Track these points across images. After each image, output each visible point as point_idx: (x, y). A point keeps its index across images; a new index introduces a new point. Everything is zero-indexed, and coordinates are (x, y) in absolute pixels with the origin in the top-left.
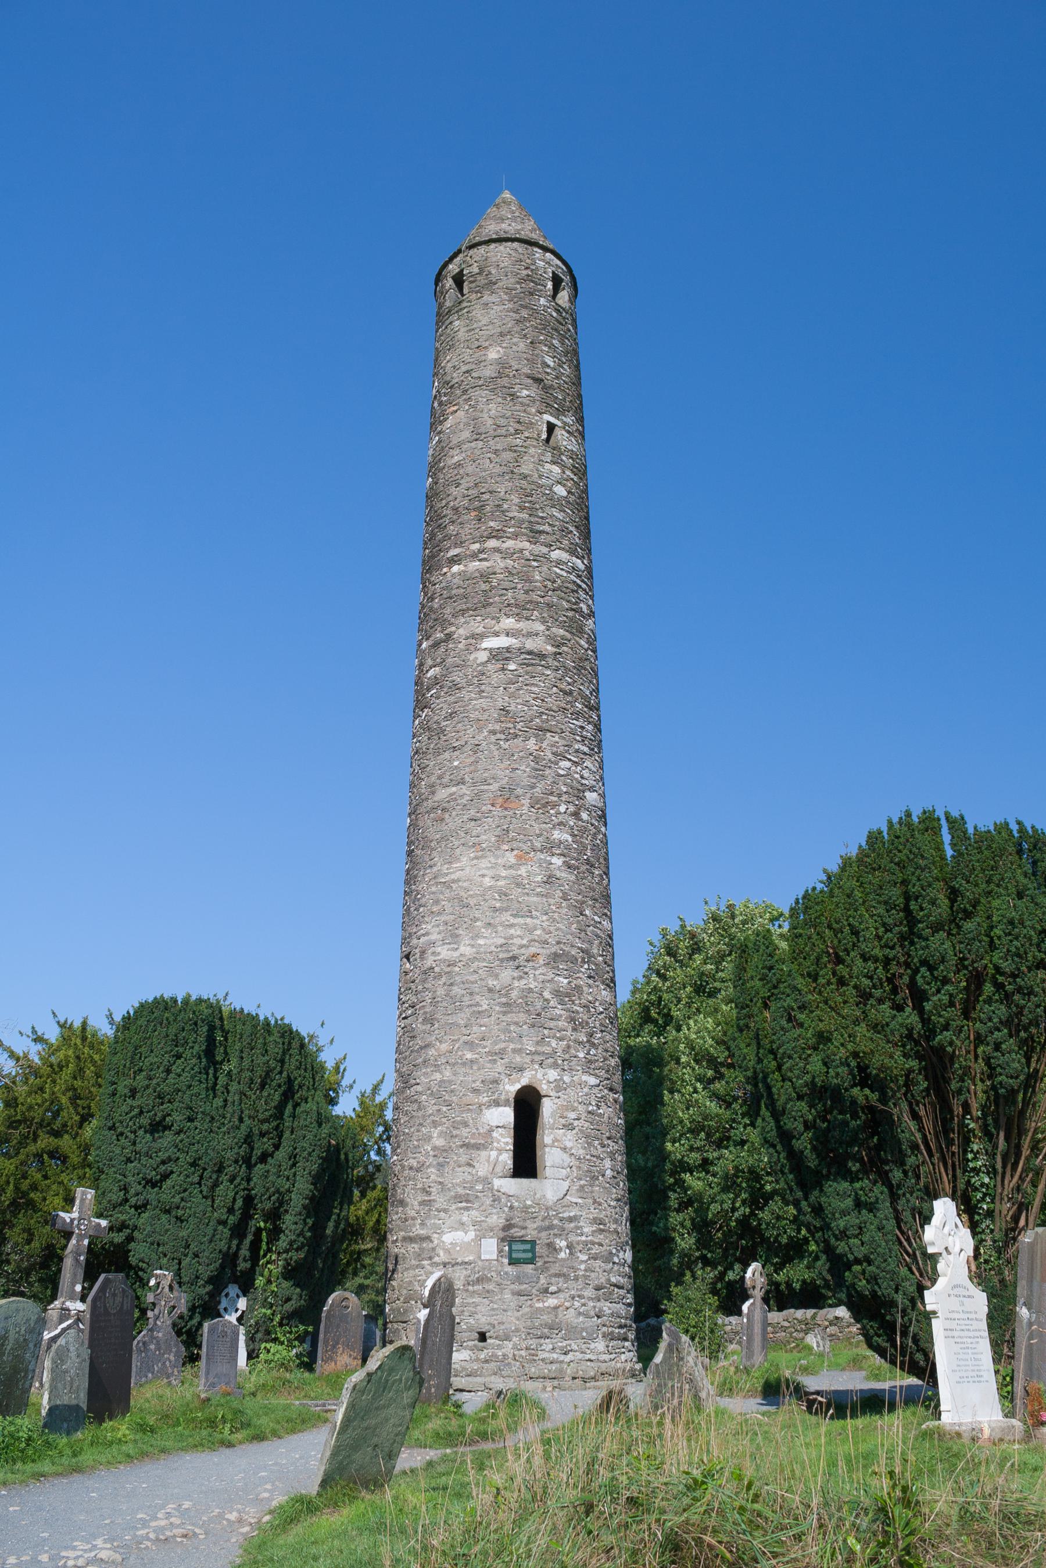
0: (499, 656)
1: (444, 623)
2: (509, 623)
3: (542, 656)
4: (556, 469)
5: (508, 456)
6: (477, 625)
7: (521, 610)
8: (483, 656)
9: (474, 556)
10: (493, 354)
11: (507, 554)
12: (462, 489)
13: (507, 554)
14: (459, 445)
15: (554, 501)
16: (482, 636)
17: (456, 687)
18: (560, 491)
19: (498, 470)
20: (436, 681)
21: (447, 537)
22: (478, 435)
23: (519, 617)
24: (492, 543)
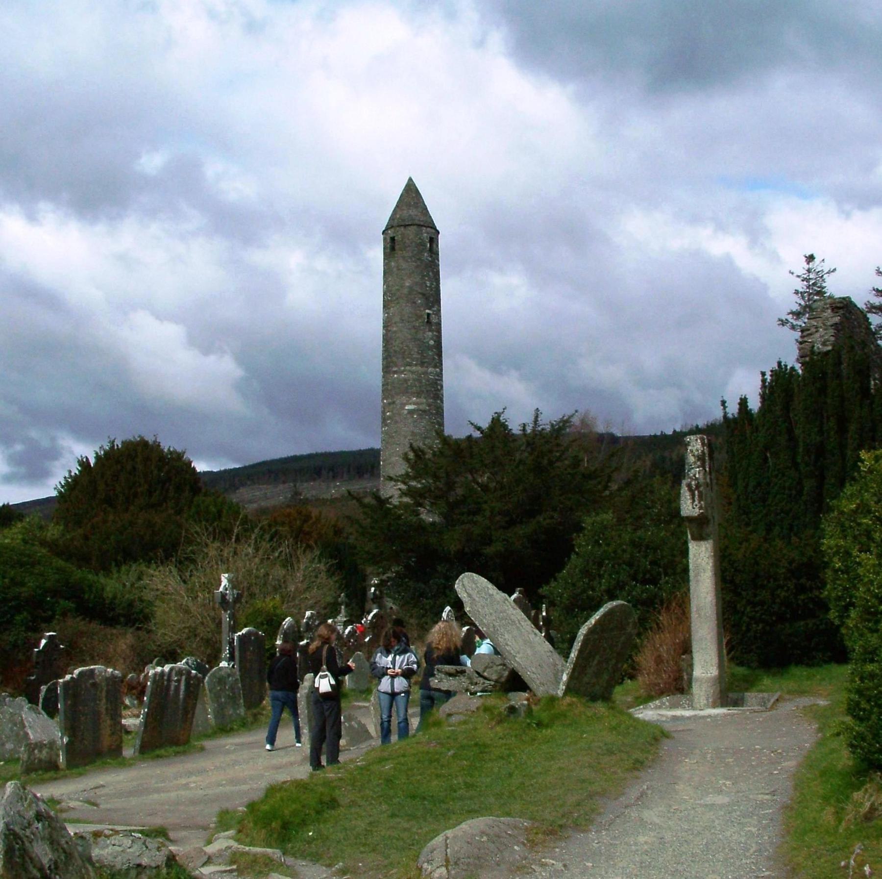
0: (411, 412)
1: (393, 397)
3: (424, 411)
4: (430, 333)
5: (413, 331)
6: (404, 399)
7: (418, 395)
8: (406, 412)
9: (402, 372)
10: (407, 284)
11: (413, 372)
13: (413, 372)
15: (430, 348)
16: (405, 404)
17: (396, 422)
18: (432, 342)
19: (410, 337)
20: (389, 418)
21: (393, 362)
22: (402, 321)
23: (418, 397)
24: (408, 368)
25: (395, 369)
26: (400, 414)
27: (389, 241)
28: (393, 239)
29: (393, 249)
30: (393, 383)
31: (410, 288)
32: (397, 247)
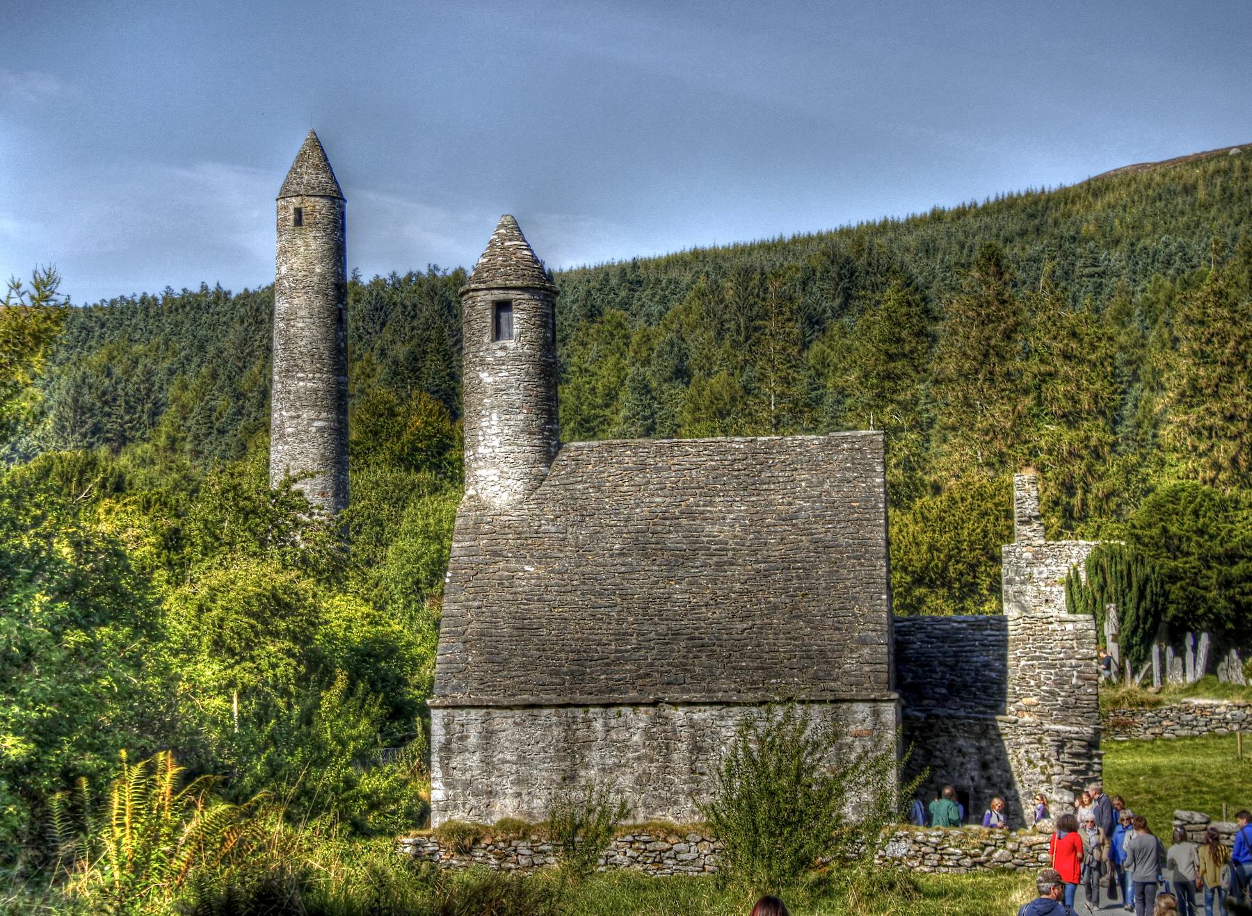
0: (319, 430)
1: (297, 409)
2: (324, 415)
6: (312, 414)
8: (314, 429)
10: (318, 270)
12: (304, 343)
14: (302, 317)
16: (314, 420)
17: (302, 441)
20: (293, 435)
24: (318, 375)
25: (300, 375)
26: (307, 432)
27: (292, 211)
28: (298, 212)
29: (298, 222)
30: (297, 391)
31: (320, 274)
32: (305, 222)
